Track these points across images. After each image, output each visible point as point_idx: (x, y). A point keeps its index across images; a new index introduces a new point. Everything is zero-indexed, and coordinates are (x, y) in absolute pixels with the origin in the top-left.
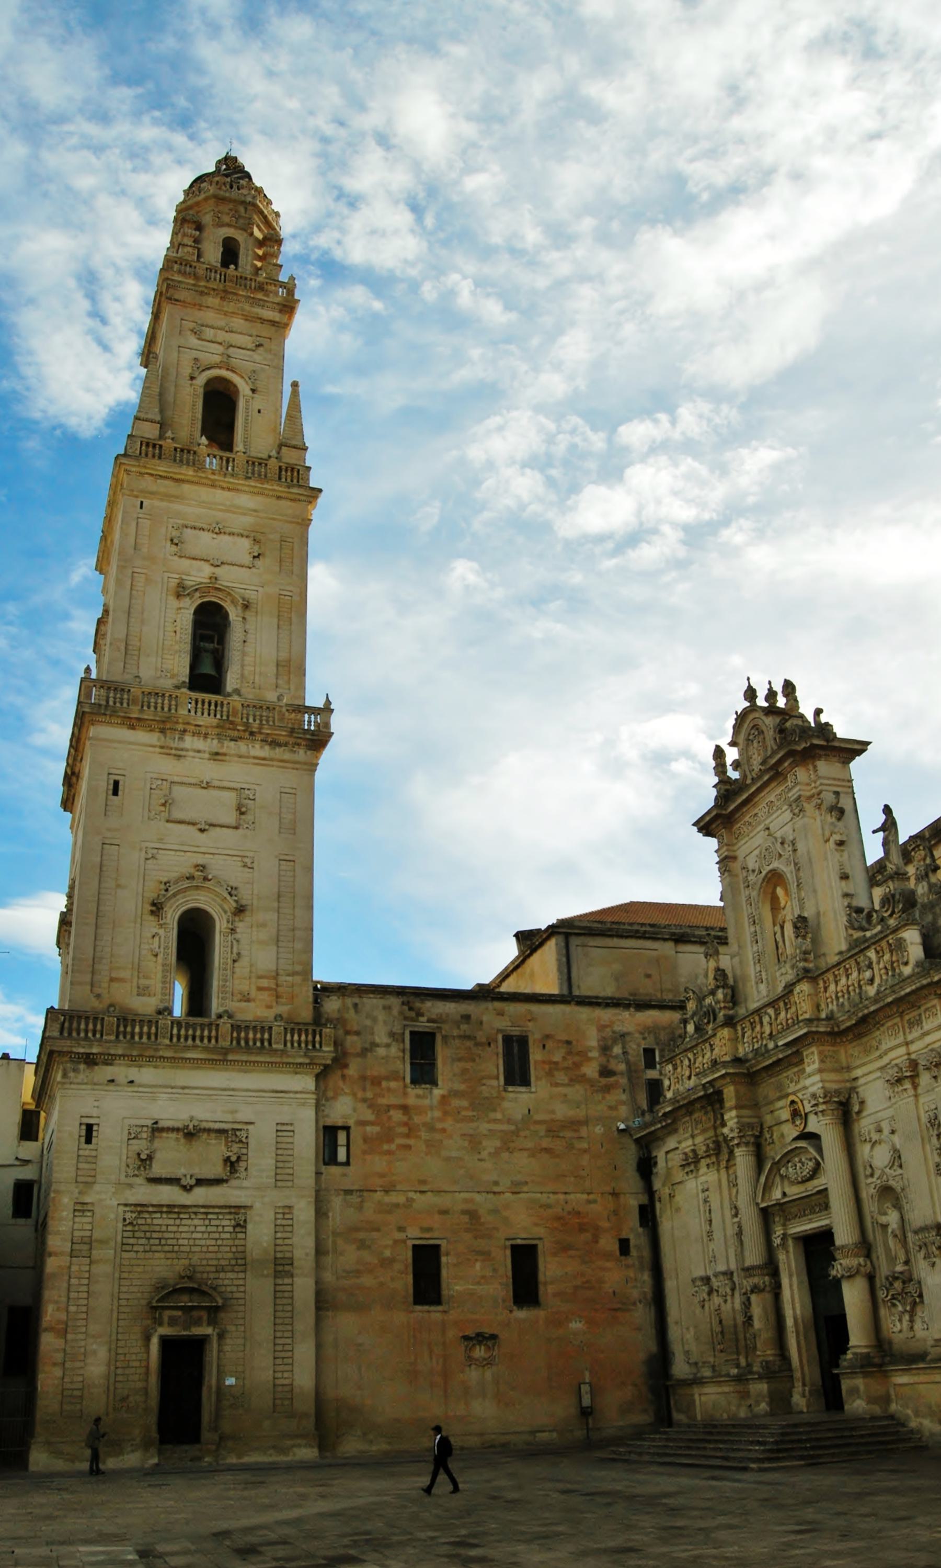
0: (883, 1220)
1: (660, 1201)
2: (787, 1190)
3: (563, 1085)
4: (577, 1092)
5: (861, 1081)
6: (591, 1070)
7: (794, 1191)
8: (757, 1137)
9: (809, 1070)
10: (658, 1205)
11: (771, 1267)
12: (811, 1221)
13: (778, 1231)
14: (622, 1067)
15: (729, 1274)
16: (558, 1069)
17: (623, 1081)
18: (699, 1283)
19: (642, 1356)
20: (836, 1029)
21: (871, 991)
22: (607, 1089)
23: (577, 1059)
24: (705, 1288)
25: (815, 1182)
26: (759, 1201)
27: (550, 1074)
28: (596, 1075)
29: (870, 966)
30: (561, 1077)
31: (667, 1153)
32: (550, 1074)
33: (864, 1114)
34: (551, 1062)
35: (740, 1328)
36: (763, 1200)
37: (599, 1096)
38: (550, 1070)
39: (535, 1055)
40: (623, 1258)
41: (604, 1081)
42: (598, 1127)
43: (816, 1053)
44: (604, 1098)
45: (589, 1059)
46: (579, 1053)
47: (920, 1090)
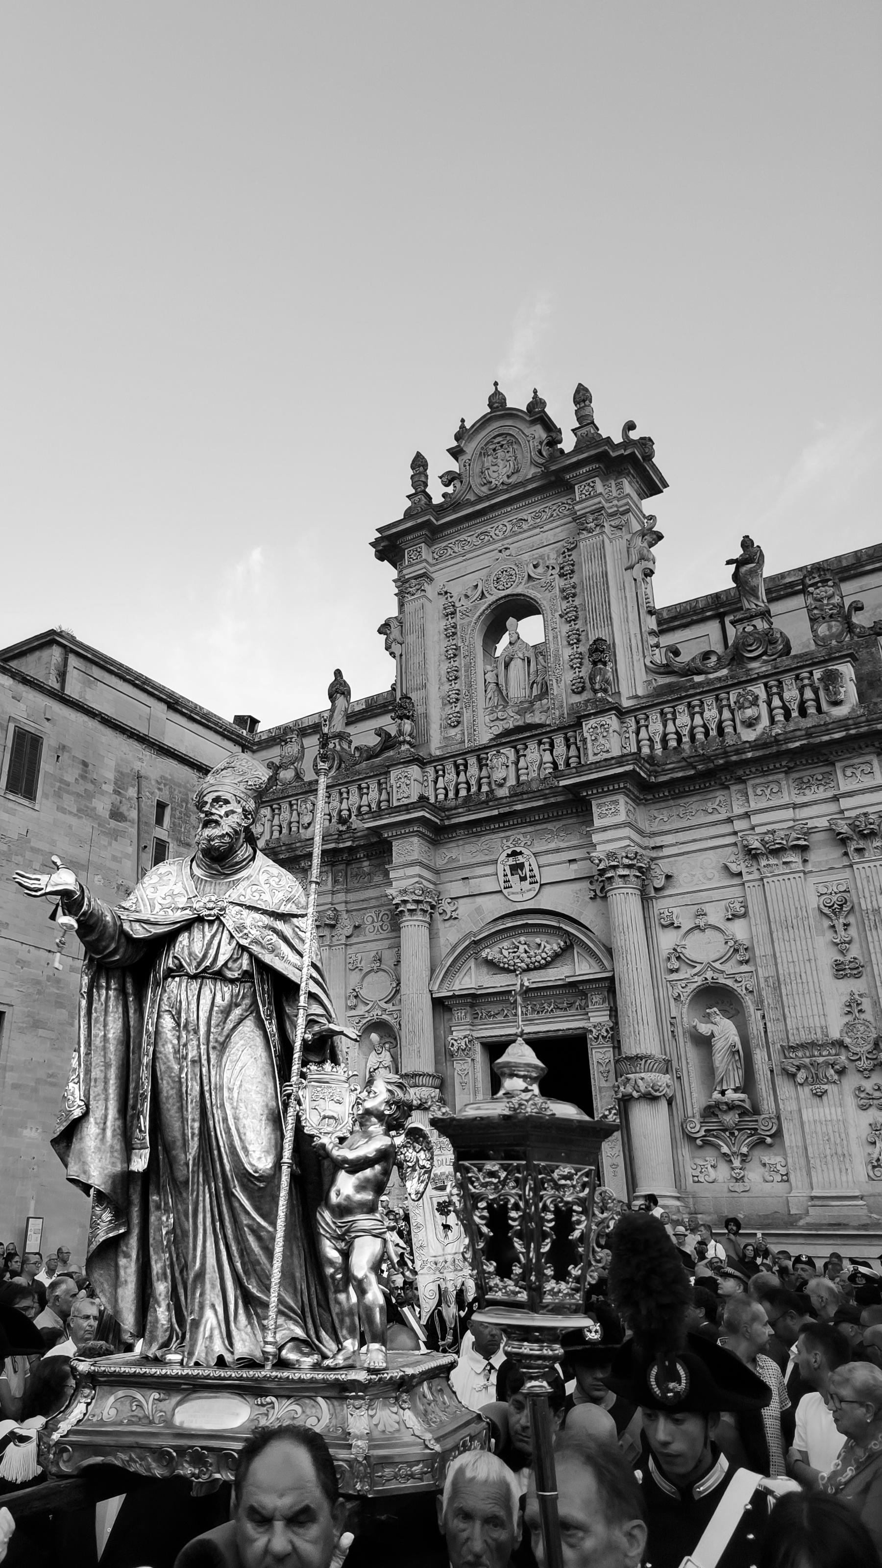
0: (704, 1029)
3: (71, 813)
4: (84, 826)
5: (666, 852)
6: (102, 806)
8: (433, 907)
9: (598, 823)
14: (134, 814)
16: (68, 792)
17: (134, 831)
20: (653, 779)
21: (749, 735)
22: (115, 835)
23: (90, 787)
26: (436, 988)
27: (58, 795)
28: (107, 814)
30: (69, 802)
32: (58, 795)
33: (667, 892)
34: (61, 781)
37: (104, 840)
38: (60, 788)
39: (46, 765)
41: (113, 823)
42: (97, 878)
44: (110, 844)
45: (103, 793)
46: (93, 782)
47: (809, 867)
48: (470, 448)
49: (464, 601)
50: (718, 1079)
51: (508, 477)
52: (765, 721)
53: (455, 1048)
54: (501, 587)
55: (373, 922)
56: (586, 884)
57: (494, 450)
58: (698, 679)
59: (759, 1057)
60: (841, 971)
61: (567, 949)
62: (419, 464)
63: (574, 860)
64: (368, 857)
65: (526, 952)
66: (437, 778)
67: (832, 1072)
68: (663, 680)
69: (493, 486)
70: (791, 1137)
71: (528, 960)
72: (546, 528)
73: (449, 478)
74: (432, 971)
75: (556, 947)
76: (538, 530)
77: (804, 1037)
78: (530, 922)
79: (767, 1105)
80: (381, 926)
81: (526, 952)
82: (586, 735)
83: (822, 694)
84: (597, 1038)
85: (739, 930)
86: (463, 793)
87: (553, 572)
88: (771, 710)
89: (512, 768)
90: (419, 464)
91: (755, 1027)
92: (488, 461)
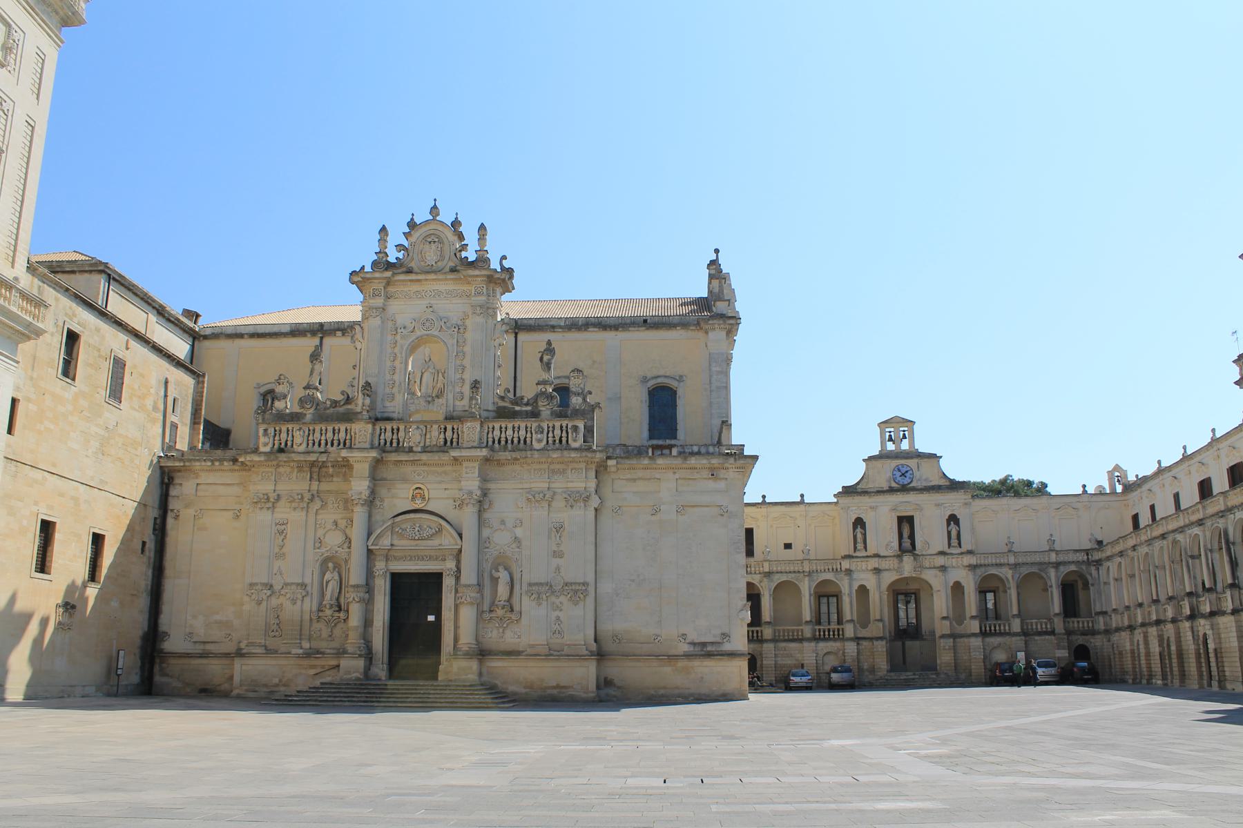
0: (496, 575)
1: (177, 517)
2: (395, 542)
7: (401, 543)
10: (170, 521)
11: (369, 587)
12: (416, 565)
13: (380, 565)
15: (303, 585)
18: (259, 587)
19: (140, 633)
24: (269, 593)
25: (430, 543)
29: (542, 432)
31: (198, 484)
35: (306, 624)
36: (372, 545)
40: (142, 556)
43: (477, 468)
48: (416, 235)
49: (402, 330)
50: (499, 595)
51: (436, 262)
52: (544, 442)
53: (377, 574)
54: (425, 329)
55: (333, 503)
56: (451, 501)
57: (430, 243)
58: (517, 408)
59: (517, 587)
60: (558, 554)
61: (440, 530)
62: (383, 230)
63: (448, 489)
64: (333, 466)
65: (418, 531)
66: (381, 433)
67: (544, 596)
68: (502, 404)
69: (427, 265)
70: (524, 621)
71: (419, 536)
72: (454, 302)
73: (400, 247)
74: (369, 535)
75: (434, 531)
76: (448, 301)
77: (536, 581)
78: (424, 517)
79: (516, 608)
80: (338, 507)
81: (418, 531)
82: (464, 430)
83: (570, 435)
84: (448, 575)
85: (519, 532)
86: (395, 444)
87: (455, 330)
88: (548, 437)
89: (423, 437)
90: (383, 230)
91: (517, 577)
92: (427, 246)
